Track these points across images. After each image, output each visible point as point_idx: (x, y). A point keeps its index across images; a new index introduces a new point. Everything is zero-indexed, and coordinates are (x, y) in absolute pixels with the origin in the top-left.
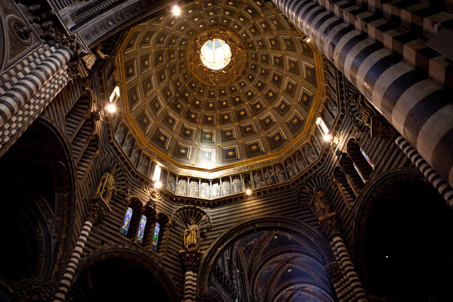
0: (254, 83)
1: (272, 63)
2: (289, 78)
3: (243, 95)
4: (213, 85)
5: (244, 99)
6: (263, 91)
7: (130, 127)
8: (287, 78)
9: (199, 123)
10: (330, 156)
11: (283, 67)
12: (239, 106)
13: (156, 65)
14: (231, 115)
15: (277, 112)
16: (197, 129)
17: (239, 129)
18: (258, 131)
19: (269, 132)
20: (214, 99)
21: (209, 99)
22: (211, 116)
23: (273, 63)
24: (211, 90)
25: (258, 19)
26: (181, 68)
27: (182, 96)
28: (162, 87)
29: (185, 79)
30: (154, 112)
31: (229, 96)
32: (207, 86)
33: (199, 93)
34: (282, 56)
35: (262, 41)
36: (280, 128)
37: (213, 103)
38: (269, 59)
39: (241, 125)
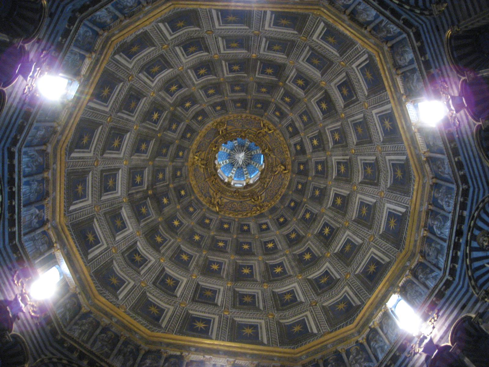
0: (285, 231)
1: (327, 204)
2: (350, 234)
3: (258, 243)
4: (214, 209)
5: (257, 248)
6: (295, 248)
7: (53, 169)
8: (348, 232)
9: (163, 254)
10: (408, 359)
11: (344, 215)
12: (244, 258)
13: (143, 121)
14: (226, 267)
15: (309, 288)
16: (156, 262)
17: (230, 294)
18: (264, 307)
19: (285, 316)
20: (206, 230)
21: (198, 227)
22: (188, 255)
23: (330, 204)
24: (207, 215)
25: (331, 123)
26: (177, 156)
27: (157, 199)
28: (133, 163)
29: (175, 176)
30: (101, 190)
31: (235, 237)
32: (203, 205)
33: (185, 209)
34: (349, 195)
35: (324, 163)
36: (308, 313)
37: (202, 237)
38: (324, 195)
39: (237, 289)
